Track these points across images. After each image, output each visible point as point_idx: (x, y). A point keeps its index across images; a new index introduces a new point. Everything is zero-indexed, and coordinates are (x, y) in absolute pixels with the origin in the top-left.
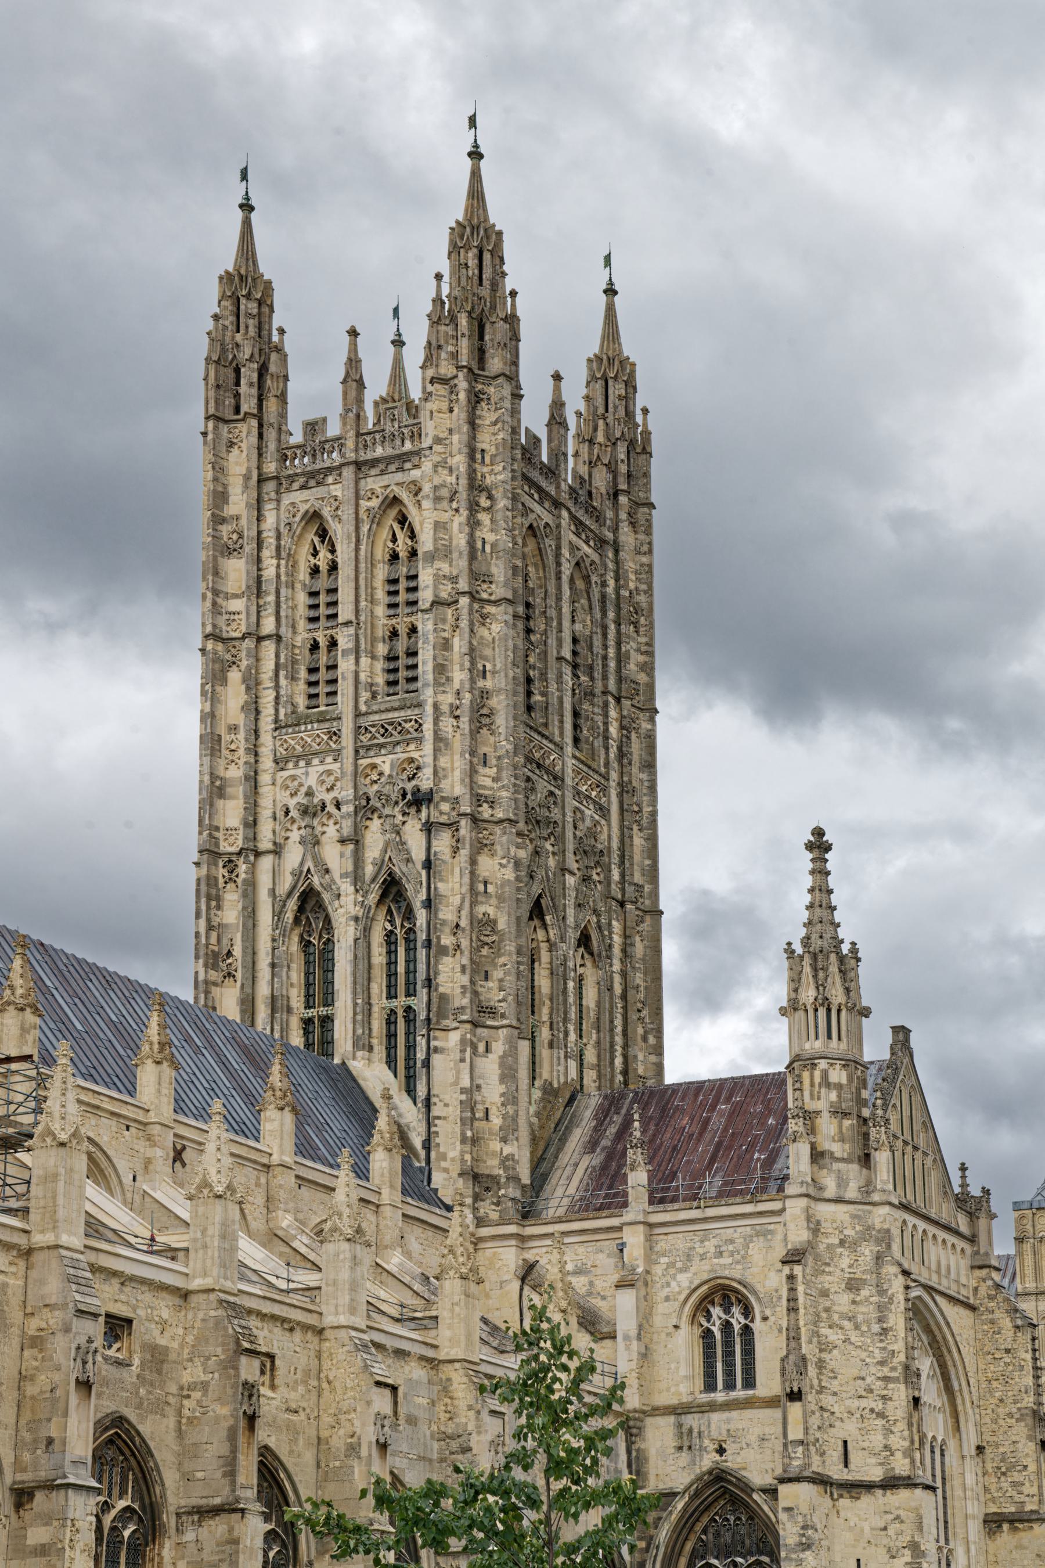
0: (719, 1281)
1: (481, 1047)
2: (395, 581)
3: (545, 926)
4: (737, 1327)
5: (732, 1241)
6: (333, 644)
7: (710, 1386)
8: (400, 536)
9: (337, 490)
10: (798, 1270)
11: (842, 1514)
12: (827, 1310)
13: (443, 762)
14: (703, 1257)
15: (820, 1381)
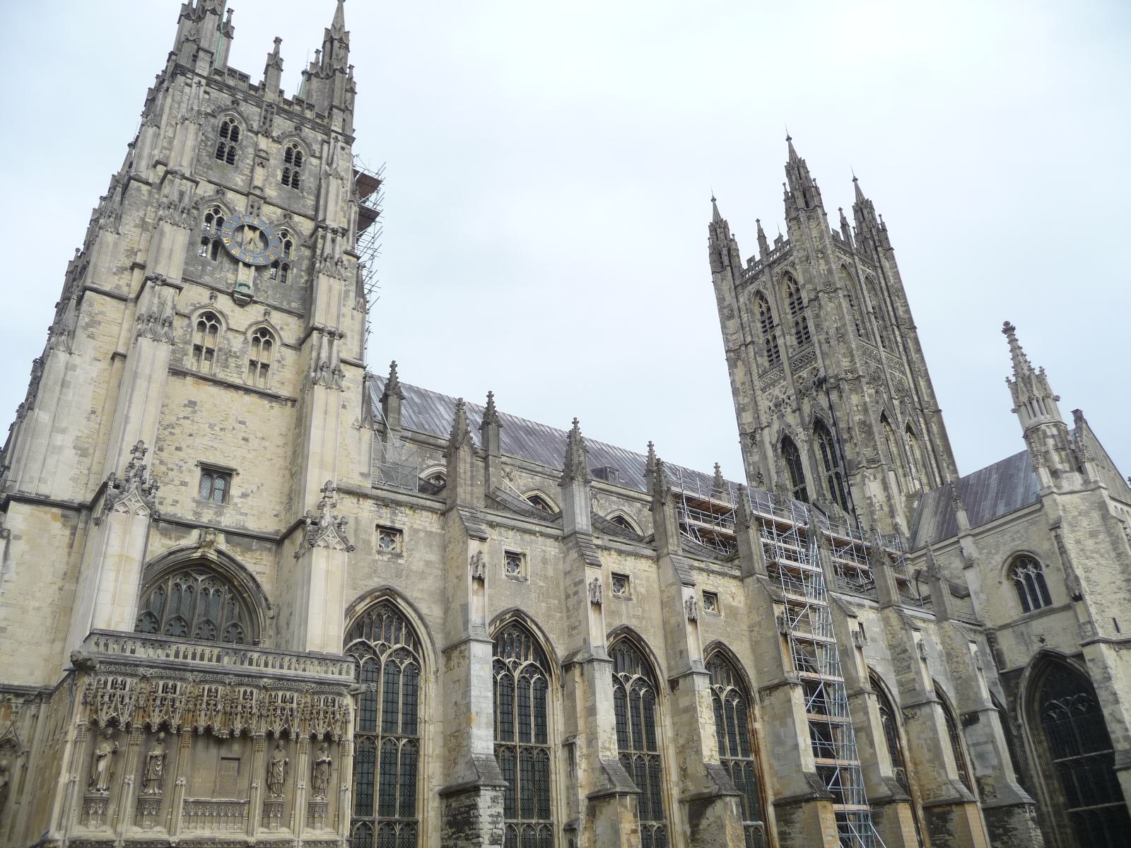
2: (793, 303)
3: (889, 424)
4: (1033, 575)
5: (1018, 532)
6: (774, 337)
7: (1026, 609)
8: (791, 286)
9: (764, 279)
12: (1082, 550)
13: (827, 362)
14: (1005, 544)
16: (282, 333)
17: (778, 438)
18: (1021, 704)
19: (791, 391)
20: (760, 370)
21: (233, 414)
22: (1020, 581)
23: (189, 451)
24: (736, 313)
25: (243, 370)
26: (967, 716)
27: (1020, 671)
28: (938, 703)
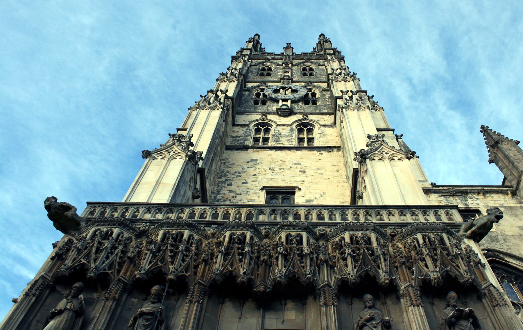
16: (319, 122)
21: (289, 161)
23: (254, 183)
25: (292, 141)
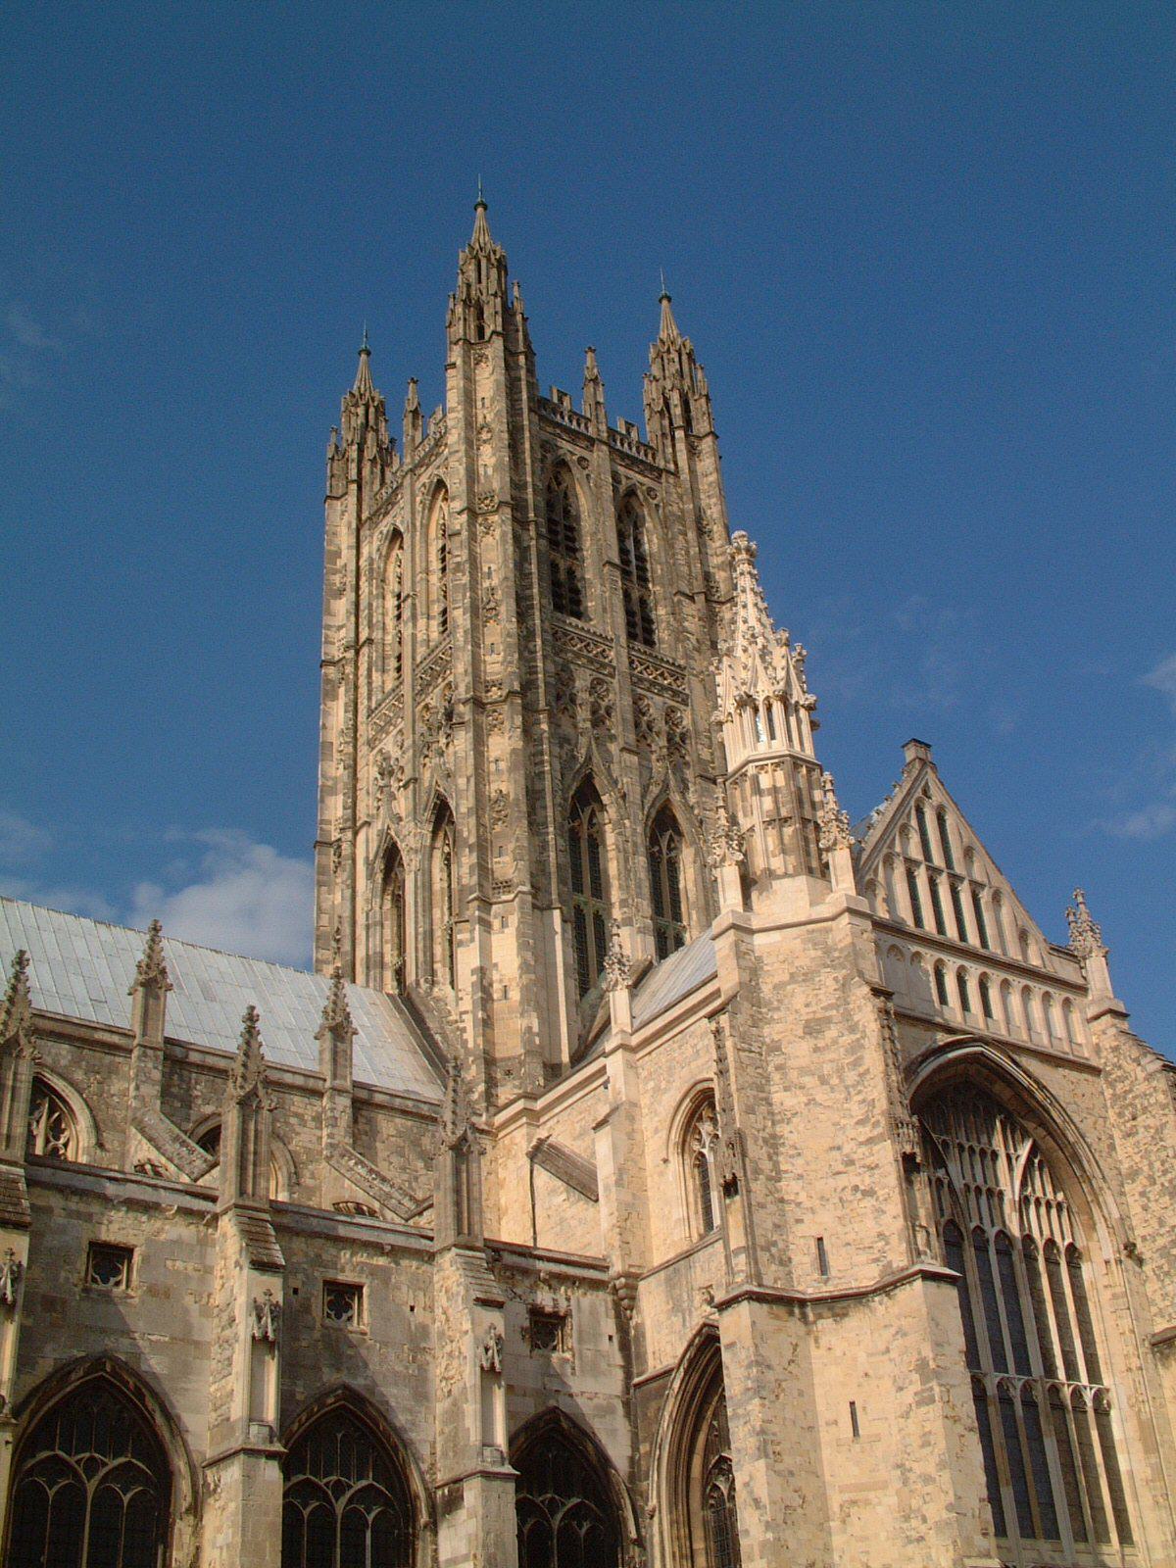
0: (699, 1087)
1: (496, 924)
10: (724, 1020)
11: (823, 1342)
12: (778, 1068)
15: (776, 1164)
17: (379, 847)
18: (659, 1459)
19: (408, 742)
20: (374, 699)
22: (702, 1155)
24: (351, 579)
26: (446, 1491)
27: (667, 1373)
28: (271, 1456)
